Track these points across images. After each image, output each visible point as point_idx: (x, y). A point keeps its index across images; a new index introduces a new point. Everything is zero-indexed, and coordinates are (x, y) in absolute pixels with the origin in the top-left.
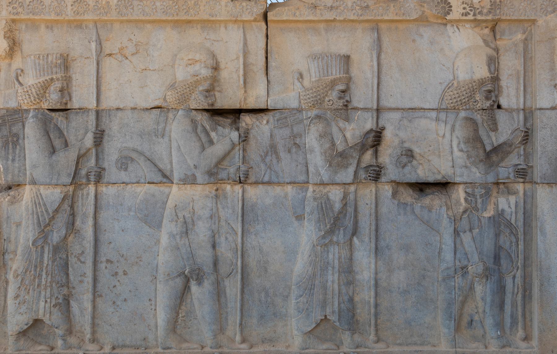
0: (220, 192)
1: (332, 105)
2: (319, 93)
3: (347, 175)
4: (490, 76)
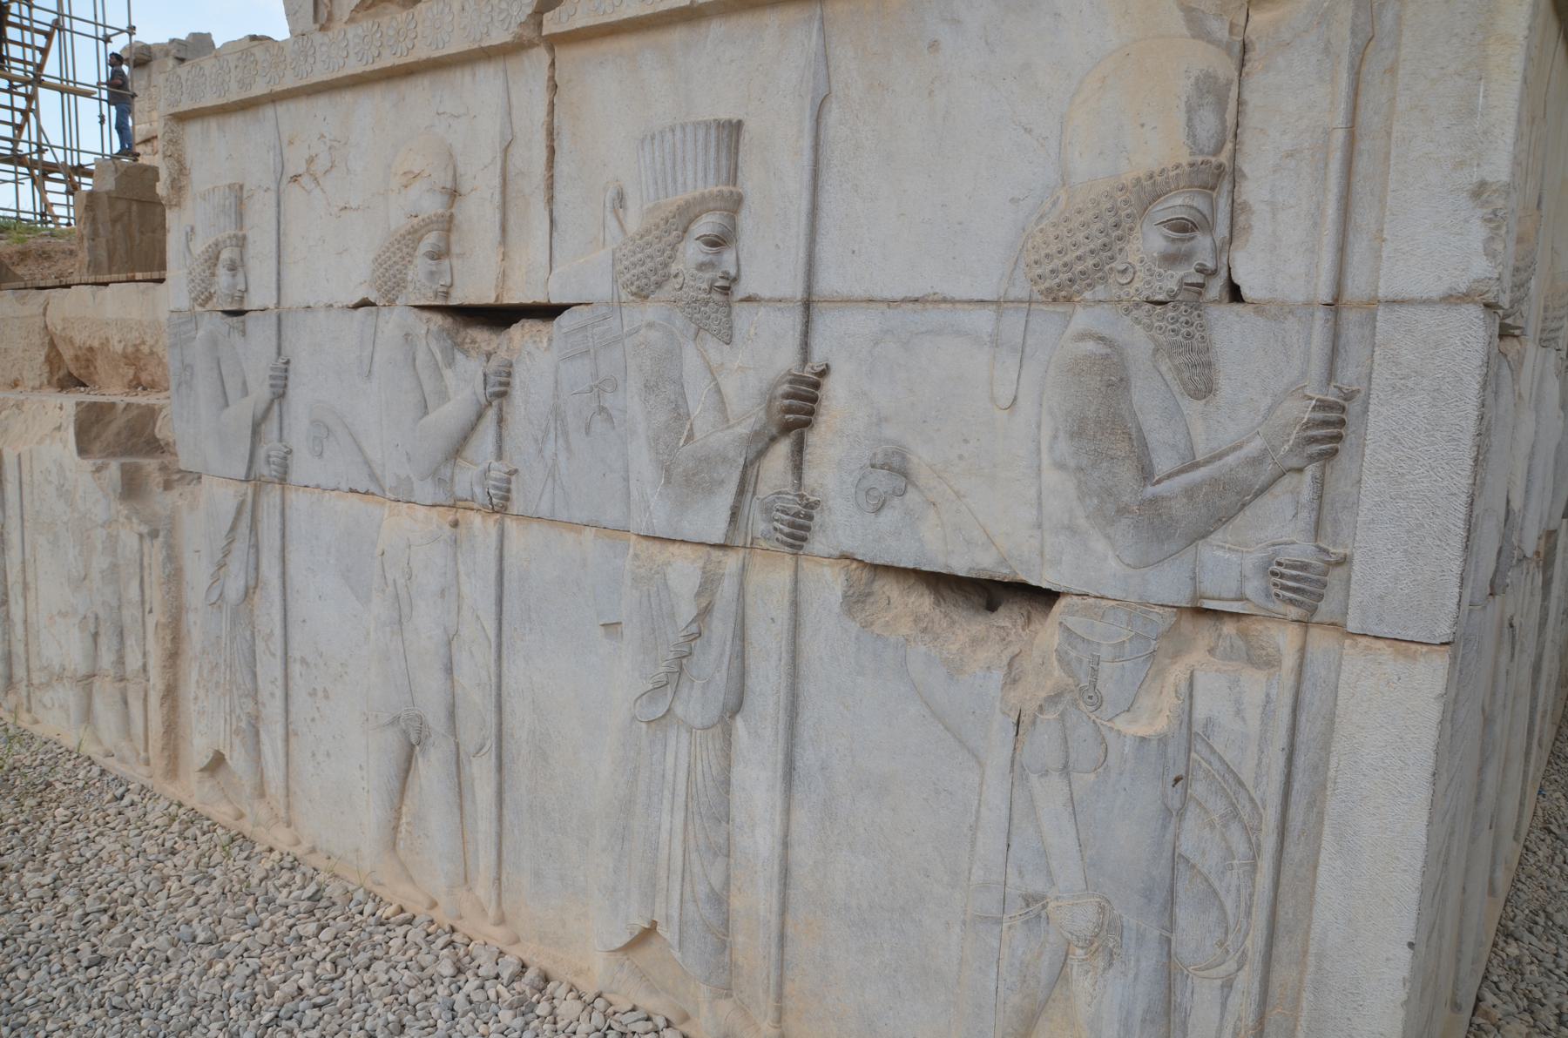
0: (462, 530)
1: (681, 288)
2: (649, 251)
3: (711, 521)
4: (1185, 159)
